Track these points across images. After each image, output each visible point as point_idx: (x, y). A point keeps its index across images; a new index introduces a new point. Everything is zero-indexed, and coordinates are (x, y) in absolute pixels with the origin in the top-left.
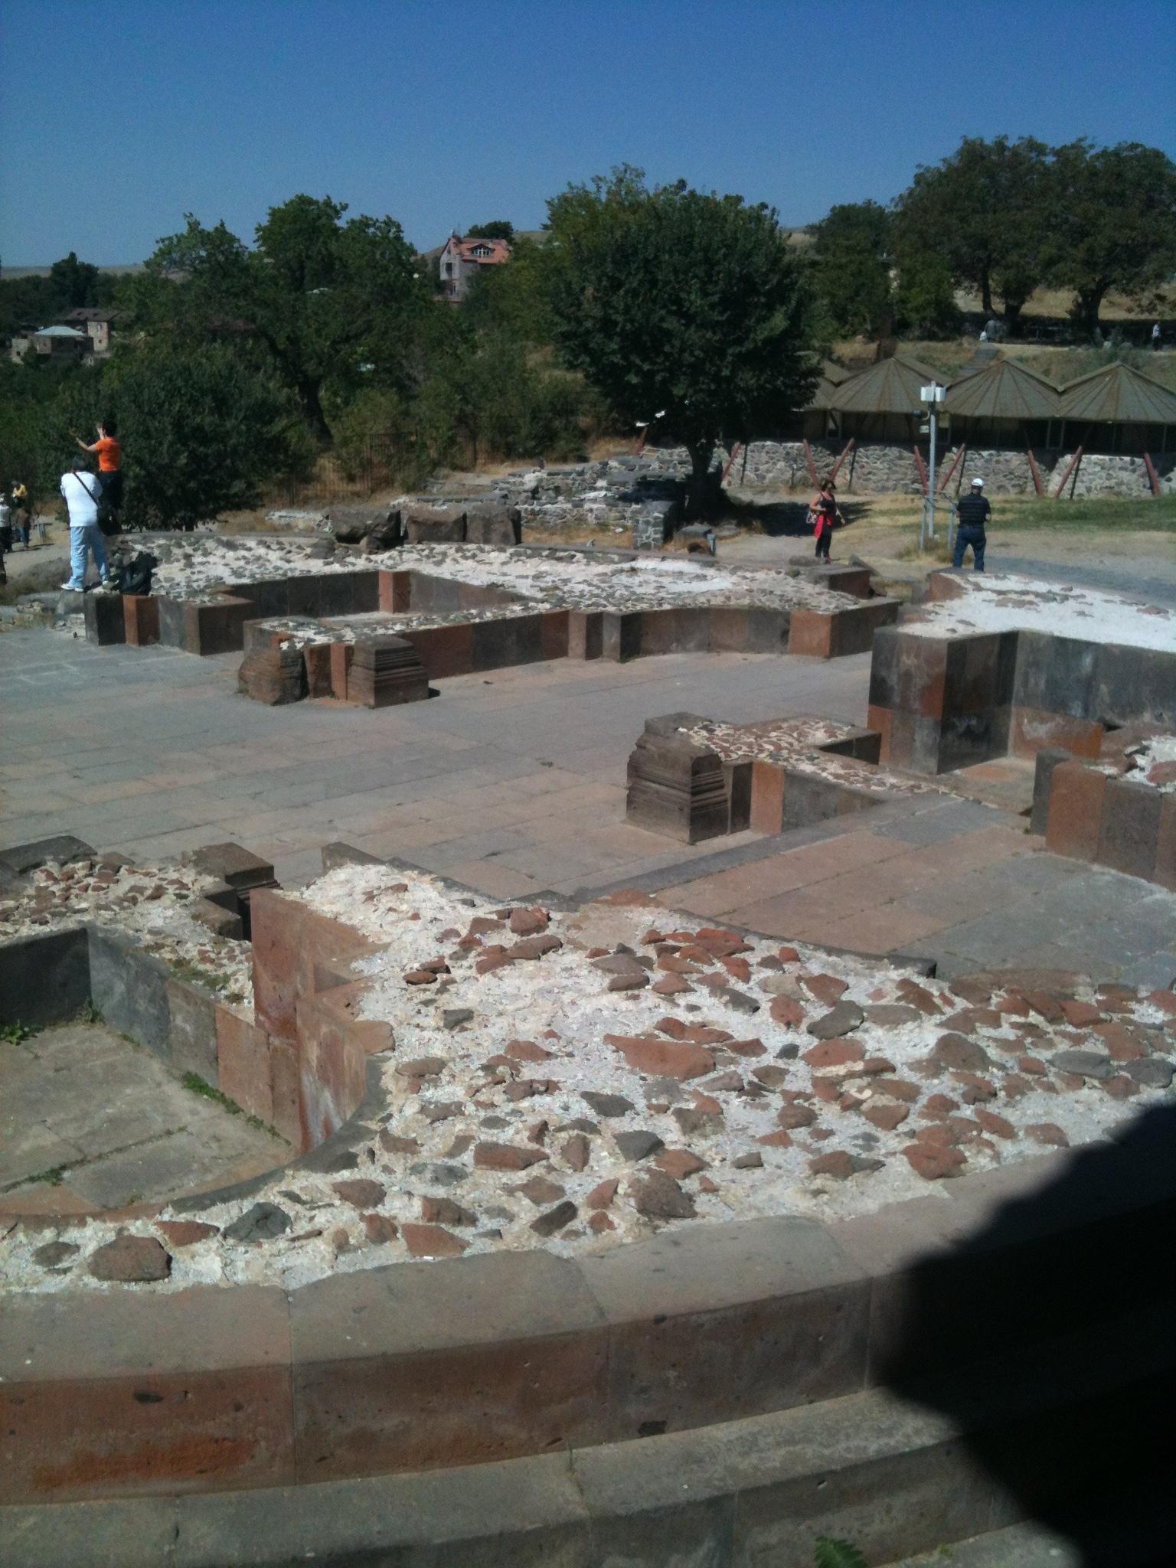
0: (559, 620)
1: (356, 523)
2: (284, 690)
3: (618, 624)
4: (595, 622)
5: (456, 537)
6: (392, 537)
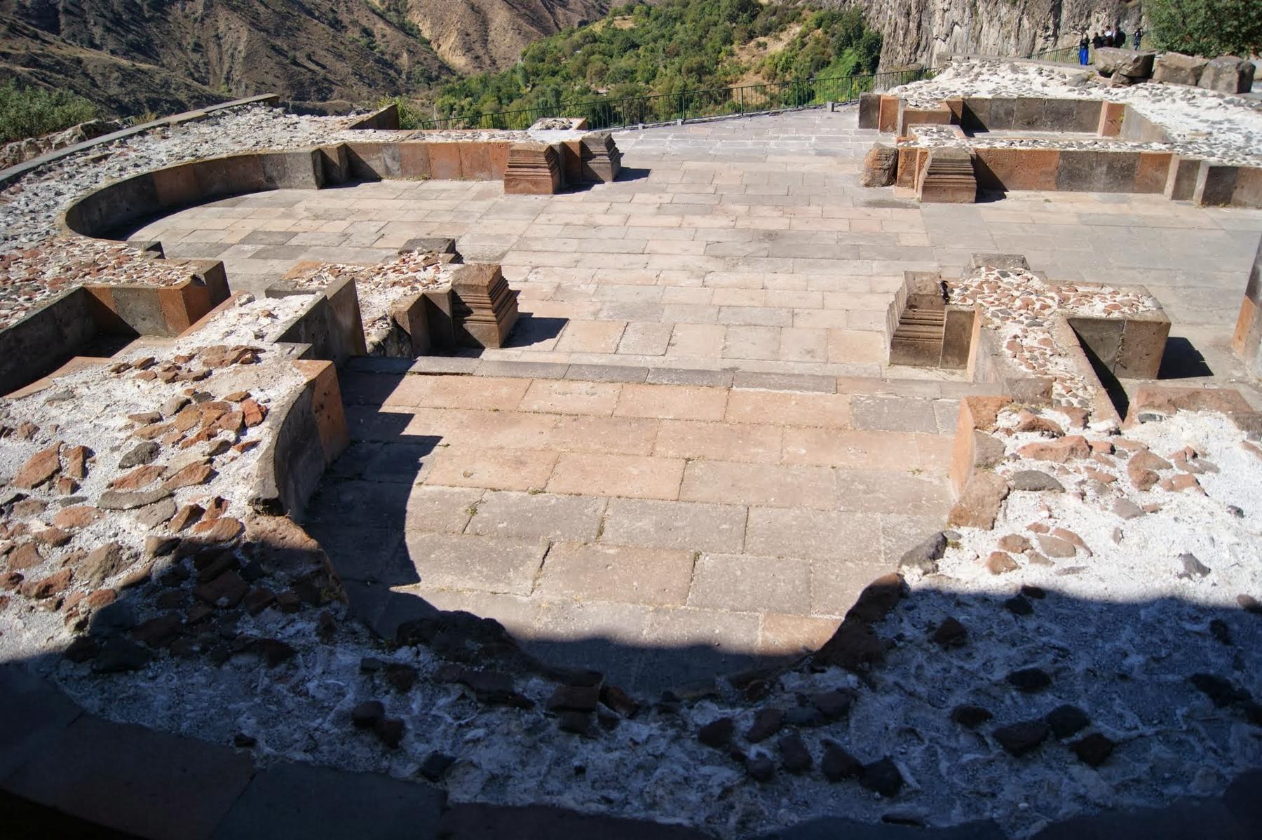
0: (1162, 161)
1: (1110, 61)
2: (873, 174)
3: (1206, 173)
4: (1189, 168)
5: (1190, 81)
6: (1142, 73)
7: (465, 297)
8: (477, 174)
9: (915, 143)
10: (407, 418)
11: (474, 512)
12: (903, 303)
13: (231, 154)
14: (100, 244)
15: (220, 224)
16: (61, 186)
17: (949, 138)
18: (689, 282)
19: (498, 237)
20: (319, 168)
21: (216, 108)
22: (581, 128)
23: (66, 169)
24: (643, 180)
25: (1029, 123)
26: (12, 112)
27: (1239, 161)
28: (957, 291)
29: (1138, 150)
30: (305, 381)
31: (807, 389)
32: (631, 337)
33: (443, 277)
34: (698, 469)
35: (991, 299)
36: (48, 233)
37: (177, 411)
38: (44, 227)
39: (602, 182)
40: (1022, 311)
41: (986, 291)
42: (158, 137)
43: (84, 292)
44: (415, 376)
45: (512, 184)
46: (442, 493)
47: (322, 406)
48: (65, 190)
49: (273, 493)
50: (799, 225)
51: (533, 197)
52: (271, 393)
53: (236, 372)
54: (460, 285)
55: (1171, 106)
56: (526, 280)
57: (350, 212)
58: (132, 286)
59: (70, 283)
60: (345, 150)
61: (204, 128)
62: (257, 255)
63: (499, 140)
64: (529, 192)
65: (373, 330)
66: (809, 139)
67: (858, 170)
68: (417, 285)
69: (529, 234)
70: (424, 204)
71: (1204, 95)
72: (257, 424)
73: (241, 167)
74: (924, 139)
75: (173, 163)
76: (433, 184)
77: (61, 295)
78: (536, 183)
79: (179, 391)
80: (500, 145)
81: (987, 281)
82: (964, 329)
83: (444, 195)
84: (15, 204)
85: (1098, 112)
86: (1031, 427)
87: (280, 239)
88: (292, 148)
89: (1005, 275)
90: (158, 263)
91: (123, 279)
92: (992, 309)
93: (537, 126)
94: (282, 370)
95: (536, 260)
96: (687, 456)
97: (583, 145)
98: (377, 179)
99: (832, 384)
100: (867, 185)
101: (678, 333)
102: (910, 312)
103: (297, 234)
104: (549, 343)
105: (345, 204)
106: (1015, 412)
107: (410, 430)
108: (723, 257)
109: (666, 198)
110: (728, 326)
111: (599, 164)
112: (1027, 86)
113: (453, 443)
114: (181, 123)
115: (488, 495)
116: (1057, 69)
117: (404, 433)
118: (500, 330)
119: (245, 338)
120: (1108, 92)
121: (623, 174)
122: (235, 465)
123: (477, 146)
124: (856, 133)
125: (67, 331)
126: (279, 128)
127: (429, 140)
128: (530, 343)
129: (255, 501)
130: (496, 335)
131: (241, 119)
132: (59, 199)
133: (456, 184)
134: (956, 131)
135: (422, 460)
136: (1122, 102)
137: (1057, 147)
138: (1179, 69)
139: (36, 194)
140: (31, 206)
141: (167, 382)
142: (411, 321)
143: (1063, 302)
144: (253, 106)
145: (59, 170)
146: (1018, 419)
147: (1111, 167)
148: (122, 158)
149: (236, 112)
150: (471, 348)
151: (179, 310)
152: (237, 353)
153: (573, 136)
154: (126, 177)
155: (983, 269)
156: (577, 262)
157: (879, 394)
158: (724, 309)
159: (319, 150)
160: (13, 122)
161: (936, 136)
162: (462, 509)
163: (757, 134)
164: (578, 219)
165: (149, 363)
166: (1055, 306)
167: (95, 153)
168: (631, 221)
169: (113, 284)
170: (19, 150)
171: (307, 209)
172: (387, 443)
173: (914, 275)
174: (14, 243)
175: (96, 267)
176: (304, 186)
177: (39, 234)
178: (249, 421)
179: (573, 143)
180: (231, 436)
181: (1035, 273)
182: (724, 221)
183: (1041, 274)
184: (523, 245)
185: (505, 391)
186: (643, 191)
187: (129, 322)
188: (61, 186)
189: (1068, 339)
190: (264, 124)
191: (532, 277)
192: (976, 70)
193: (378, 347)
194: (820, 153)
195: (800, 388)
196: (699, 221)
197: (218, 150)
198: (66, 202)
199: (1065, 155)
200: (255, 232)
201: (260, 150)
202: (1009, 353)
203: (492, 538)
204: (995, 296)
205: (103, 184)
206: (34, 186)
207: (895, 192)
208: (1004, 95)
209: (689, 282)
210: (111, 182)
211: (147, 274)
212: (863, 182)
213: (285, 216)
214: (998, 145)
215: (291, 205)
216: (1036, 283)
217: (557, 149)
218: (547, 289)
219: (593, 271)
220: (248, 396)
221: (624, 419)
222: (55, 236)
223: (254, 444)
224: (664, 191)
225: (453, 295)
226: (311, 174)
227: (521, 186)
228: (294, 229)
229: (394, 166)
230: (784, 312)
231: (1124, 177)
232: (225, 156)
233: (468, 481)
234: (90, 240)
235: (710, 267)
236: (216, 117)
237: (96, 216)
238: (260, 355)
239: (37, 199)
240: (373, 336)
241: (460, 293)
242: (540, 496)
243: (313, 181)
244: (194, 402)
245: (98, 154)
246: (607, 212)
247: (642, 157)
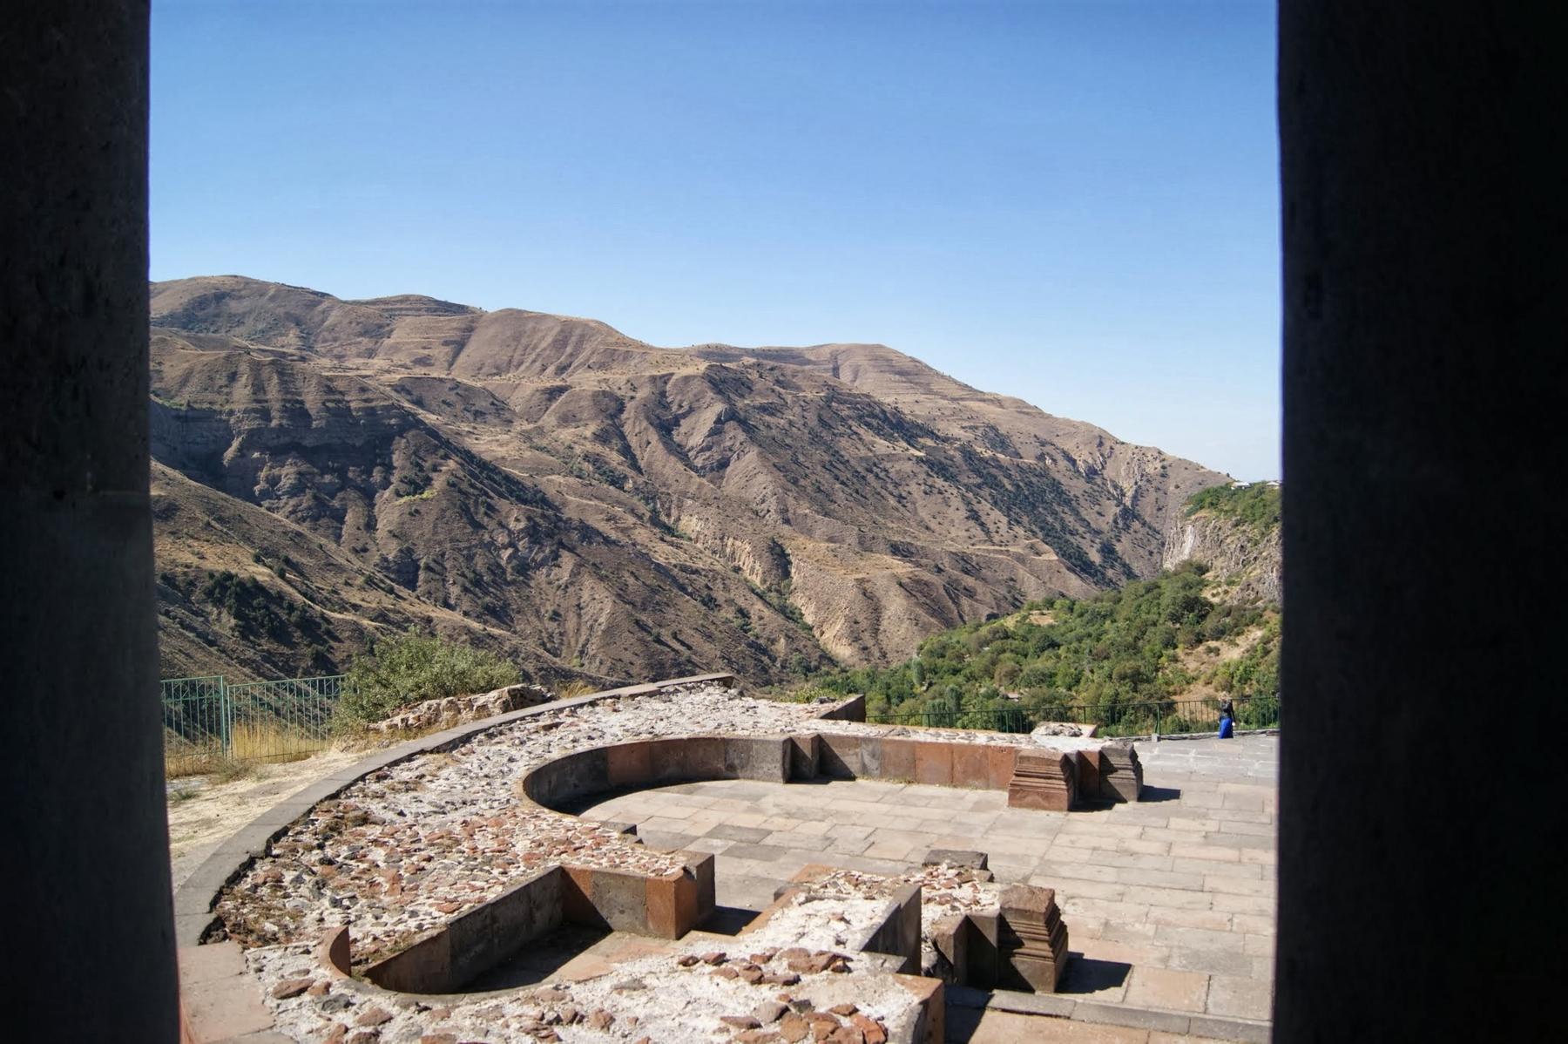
7: (1016, 924)
13: (691, 735)
20: (788, 760)
21: (669, 684)
22: (1094, 735)
23: (517, 734)
24: (1174, 802)
26: (436, 669)
30: (917, 1000)
33: (985, 898)
38: (502, 794)
39: (1125, 801)
42: (609, 709)
43: (562, 872)
44: (997, 1013)
45: (1018, 796)
48: (517, 757)
51: (1044, 813)
53: (832, 982)
60: (819, 741)
61: (656, 704)
63: (1000, 743)
64: (1035, 806)
69: (1051, 856)
70: (912, 811)
73: (701, 752)
75: (628, 740)
76: (915, 789)
77: (536, 874)
78: (1047, 797)
79: (770, 995)
80: (1001, 750)
83: (934, 802)
84: (468, 766)
87: (752, 837)
88: (758, 734)
97: (1102, 755)
98: (852, 778)
105: (819, 803)
111: (1120, 780)
114: (633, 696)
121: (1148, 794)
123: (975, 748)
125: (538, 915)
126: (737, 711)
127: (914, 737)
128: (1091, 991)
130: (1051, 976)
131: (697, 697)
140: (486, 771)
141: (753, 983)
148: (574, 729)
151: (665, 906)
154: (580, 749)
156: (1122, 894)
167: (545, 720)
168: (1175, 851)
170: (437, 709)
171: (776, 805)
174: (474, 809)
176: (769, 778)
187: (604, 913)
188: (513, 752)
197: (676, 729)
198: (521, 770)
201: (715, 734)
205: (556, 754)
211: (631, 860)
217: (1074, 759)
218: (1093, 925)
219: (1144, 909)
220: (856, 1010)
224: (1205, 816)
225: (1001, 920)
226: (779, 765)
227: (1029, 799)
229: (873, 765)
234: (557, 815)
236: (669, 693)
241: (1009, 919)
243: (779, 773)
244: (793, 1010)
245: (549, 722)
246: (1140, 837)
247: (1164, 774)
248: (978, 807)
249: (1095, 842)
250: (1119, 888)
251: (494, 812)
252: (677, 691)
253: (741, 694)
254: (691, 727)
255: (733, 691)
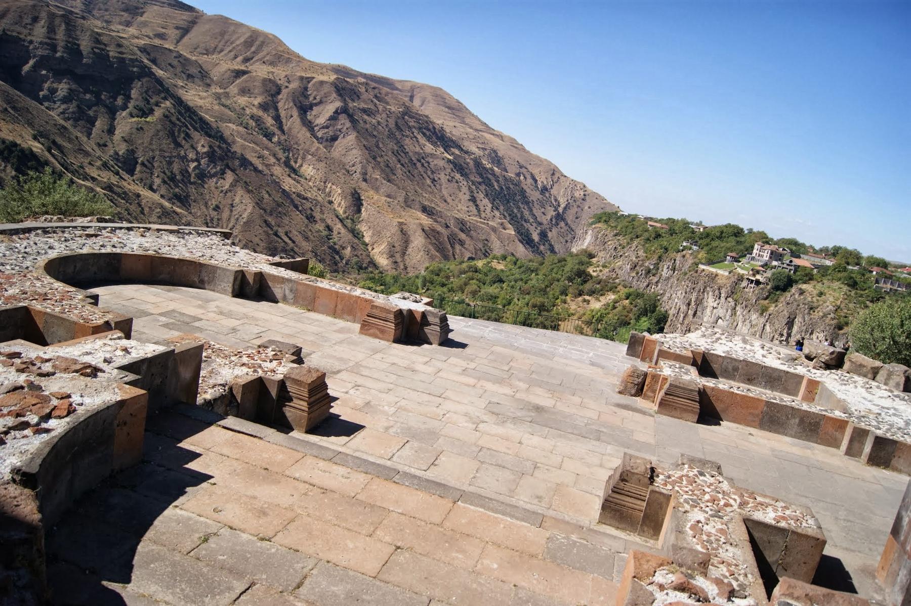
0: (841, 425)
1: (813, 350)
2: (626, 387)
3: (873, 440)
4: (860, 434)
6: (836, 363)
7: (291, 388)
8: (345, 316)
9: (661, 371)
10: (195, 456)
11: (206, 540)
12: (617, 476)
14: (58, 285)
15: (153, 299)
16: (56, 244)
17: (686, 374)
18: (466, 424)
19: (341, 359)
20: (238, 282)
22: (427, 304)
23: (66, 235)
25: (749, 380)
27: (898, 437)
28: (661, 477)
29: (824, 413)
30: (119, 399)
31: (517, 519)
32: (407, 451)
34: (401, 558)
35: (687, 489)
36: (27, 268)
37: (9, 392)
38: (28, 264)
39: (430, 344)
40: (709, 504)
41: (685, 482)
43: (26, 310)
44: (219, 428)
45: (365, 328)
46: (190, 519)
47: (125, 424)
49: (34, 469)
50: (560, 407)
51: (378, 340)
52: (87, 400)
53: (73, 379)
54: (289, 378)
55: (854, 390)
56: (347, 393)
57: (246, 316)
58: (61, 315)
59: (20, 302)
60: (260, 276)
61: (173, 238)
62: (166, 326)
64: (376, 337)
65: (210, 391)
66: (588, 353)
67: (617, 382)
68: (259, 370)
69: (364, 363)
70: (299, 325)
71: (878, 387)
72: (60, 417)
73: (185, 268)
74: (667, 370)
75: (140, 252)
76: (313, 315)
77: (9, 306)
78: (382, 332)
80: (366, 300)
81: (687, 476)
82: (661, 508)
84: (18, 245)
85: (800, 383)
86: (681, 588)
87: (187, 320)
88: (224, 265)
89: (702, 474)
90: (89, 307)
91: (57, 309)
92: (685, 496)
93: (399, 295)
94: (106, 388)
95: (360, 381)
96: (399, 544)
97: (424, 314)
98: (275, 301)
99: (540, 521)
100: (620, 392)
101: (443, 458)
102: (622, 484)
103: (201, 320)
104: (343, 439)
105: (244, 310)
106: (672, 573)
107: (193, 466)
108: (497, 414)
109: (472, 365)
110: (482, 463)
111: (433, 331)
112: (752, 354)
113: (221, 484)
114: (158, 230)
115: (225, 532)
116: (775, 348)
117: (186, 466)
118: (309, 419)
119: (96, 360)
120: (809, 371)
121: (447, 342)
122: (24, 441)
124: (623, 357)
127: (320, 285)
129: (16, 471)
130: (304, 422)
131: (200, 239)
132: (50, 251)
133: (329, 319)
134: (693, 371)
135: (188, 489)
136: (818, 379)
137: (764, 398)
138: (861, 366)
139: (36, 244)
140: (27, 250)
141: (18, 371)
142: (243, 394)
143: (742, 505)
144: (212, 234)
145: (60, 234)
146: (672, 578)
147: (802, 421)
148: (107, 240)
149: (199, 234)
150: (285, 427)
152: (82, 366)
153: (419, 308)
154: (103, 251)
155: (686, 466)
157: (574, 537)
158: (485, 450)
159: (242, 271)
160: (55, 204)
161: (677, 370)
162: (197, 535)
163: (552, 342)
164: (405, 363)
165: (17, 355)
166: (736, 507)
167: (90, 231)
168: (440, 374)
169: (48, 310)
171: (217, 307)
172: (168, 469)
173: (631, 457)
175: (45, 297)
176: (223, 292)
177: (21, 267)
178: (54, 414)
179: (417, 312)
180: (33, 419)
181: (727, 478)
182: (507, 391)
183: (731, 480)
184: (356, 369)
185: (280, 457)
186: (456, 356)
188: (56, 244)
189: (740, 533)
190: (214, 247)
191: (352, 392)
192: (718, 335)
193: (208, 403)
194: (593, 364)
195: (512, 516)
196: (489, 386)
197: (174, 253)
198: (53, 254)
199: (769, 404)
200: (173, 311)
201: (202, 260)
202: (691, 532)
203: (208, 565)
204: (691, 487)
205: (85, 251)
206: (37, 239)
207: (639, 402)
208: (734, 356)
209: (466, 424)
210: (91, 251)
211: (75, 311)
212: (617, 390)
213: (200, 307)
214: (721, 386)
215: (208, 301)
216: (725, 486)
217: (405, 313)
218: (360, 402)
219: (397, 399)
220: (69, 396)
221: (361, 503)
222: (31, 271)
223: (47, 431)
225: (282, 384)
226: (231, 285)
227: (371, 331)
228: (202, 317)
229: (290, 296)
230: (529, 464)
231: (811, 430)
232: (176, 257)
233: (215, 515)
234: (52, 280)
235: (485, 418)
237: (70, 270)
238: (99, 374)
239: (34, 247)
240: (207, 393)
242: (266, 544)
243: (230, 290)
244: (26, 389)
245: (93, 233)
247: (466, 335)
248: (341, 331)
249: (396, 360)
250: (391, 386)
251: (14, 272)
252: (190, 233)
253: (233, 244)
254: (184, 253)
255: (229, 242)
